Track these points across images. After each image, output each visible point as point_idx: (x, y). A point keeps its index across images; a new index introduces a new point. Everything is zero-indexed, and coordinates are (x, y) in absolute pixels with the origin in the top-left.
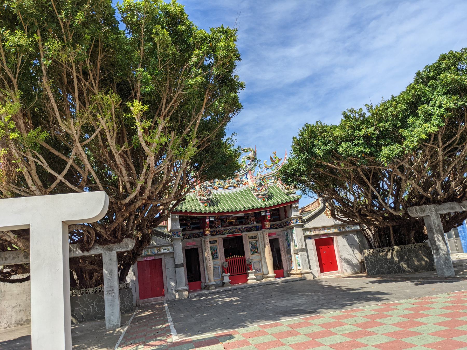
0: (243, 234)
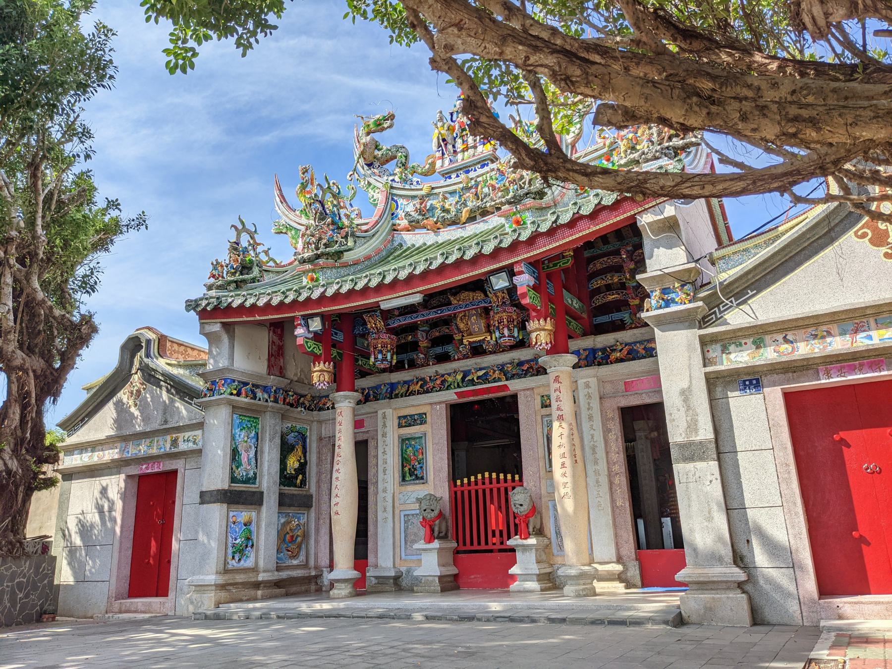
0: (515, 385)
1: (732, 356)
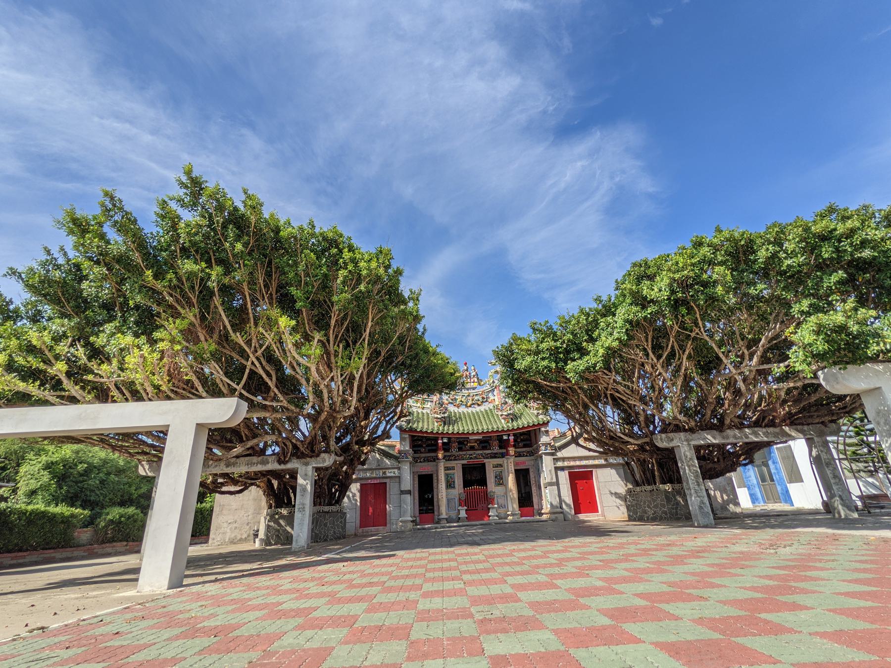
0: (486, 461)
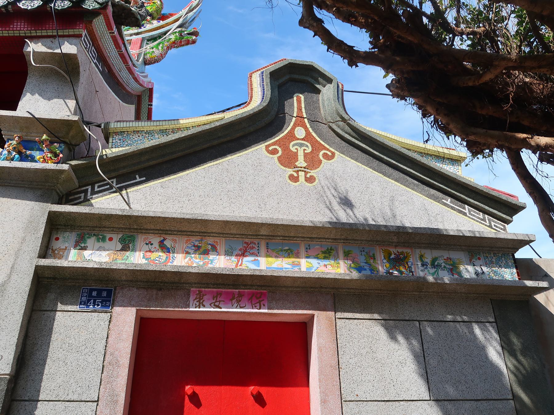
1: (87, 253)
